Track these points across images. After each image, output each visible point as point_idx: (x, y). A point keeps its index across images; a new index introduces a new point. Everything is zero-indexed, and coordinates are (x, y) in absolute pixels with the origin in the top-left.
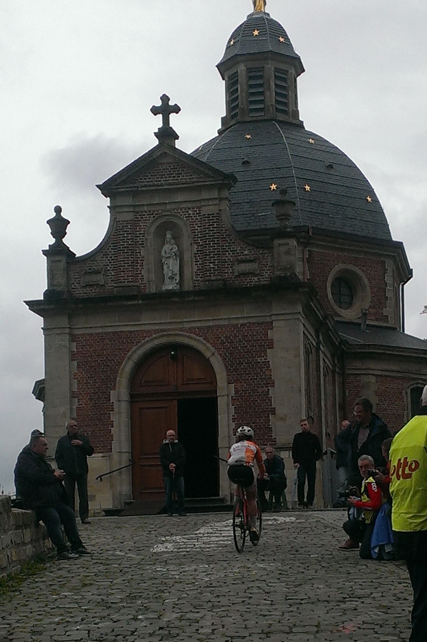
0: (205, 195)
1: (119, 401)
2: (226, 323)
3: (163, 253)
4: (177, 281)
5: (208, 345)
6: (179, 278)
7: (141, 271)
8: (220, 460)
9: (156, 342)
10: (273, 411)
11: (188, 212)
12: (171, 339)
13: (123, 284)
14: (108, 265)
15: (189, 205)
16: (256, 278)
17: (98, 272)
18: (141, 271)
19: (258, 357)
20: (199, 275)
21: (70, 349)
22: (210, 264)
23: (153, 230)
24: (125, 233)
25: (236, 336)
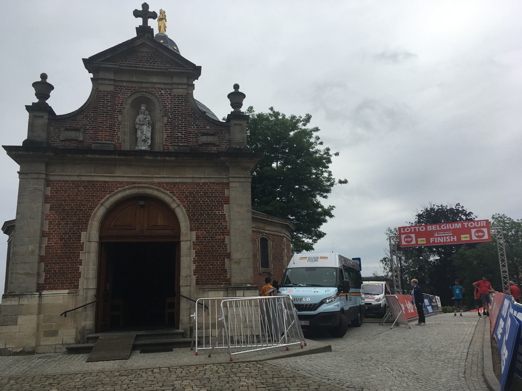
0: (176, 80)
1: (89, 241)
2: (189, 180)
3: (137, 120)
4: (149, 144)
5: (174, 198)
6: (150, 142)
8: (181, 297)
9: (128, 192)
10: (229, 256)
11: (161, 91)
12: (141, 191)
13: (101, 142)
14: (88, 125)
15: (162, 86)
17: (77, 130)
18: (117, 133)
19: (216, 210)
20: (168, 141)
21: (44, 193)
22: (179, 134)
23: (130, 101)
24: (106, 101)
25: (198, 192)
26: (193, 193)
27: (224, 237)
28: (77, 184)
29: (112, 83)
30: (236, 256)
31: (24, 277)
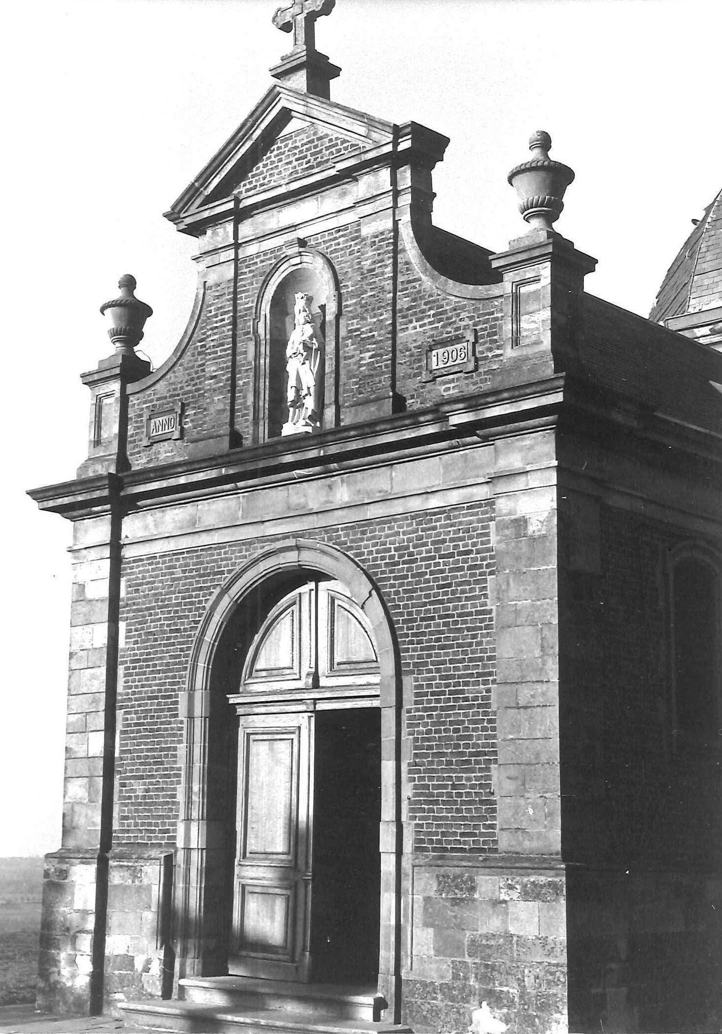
26: (407, 548)
27: (488, 691)
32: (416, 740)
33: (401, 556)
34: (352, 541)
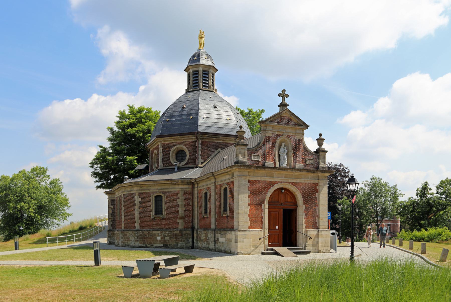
7: (274, 157)
16: (313, 166)
24: (269, 141)
26: (304, 187)
28: (259, 182)
29: (272, 132)
30: (321, 216)
31: (243, 223)
32: (305, 214)
33: (303, 188)
34: (295, 185)
